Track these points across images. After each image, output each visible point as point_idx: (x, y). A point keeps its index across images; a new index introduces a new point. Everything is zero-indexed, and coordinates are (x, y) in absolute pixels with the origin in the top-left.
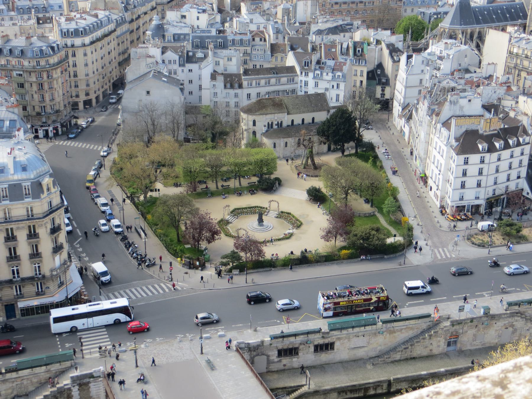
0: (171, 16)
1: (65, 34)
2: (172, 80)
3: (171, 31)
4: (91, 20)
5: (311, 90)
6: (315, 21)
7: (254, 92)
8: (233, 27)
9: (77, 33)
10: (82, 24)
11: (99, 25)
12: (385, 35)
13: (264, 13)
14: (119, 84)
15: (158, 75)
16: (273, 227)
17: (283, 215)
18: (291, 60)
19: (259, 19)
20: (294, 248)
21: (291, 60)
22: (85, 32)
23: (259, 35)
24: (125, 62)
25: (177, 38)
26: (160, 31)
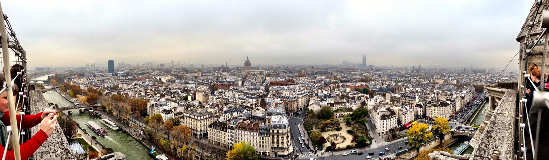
0: (320, 91)
1: (298, 94)
2: (319, 105)
3: (319, 94)
4: (303, 92)
5: (349, 107)
6: (350, 92)
7: (337, 108)
8: (333, 93)
9: (300, 94)
10: (301, 93)
11: (305, 93)
12: (366, 95)
13: (339, 90)
14: (308, 105)
15: (316, 103)
16: (340, 140)
17: (341, 137)
18: (345, 100)
19: (338, 92)
20: (344, 145)
21: (345, 100)
22: (302, 94)
23: (339, 95)
24: (309, 101)
25: (321, 96)
26: (317, 94)
